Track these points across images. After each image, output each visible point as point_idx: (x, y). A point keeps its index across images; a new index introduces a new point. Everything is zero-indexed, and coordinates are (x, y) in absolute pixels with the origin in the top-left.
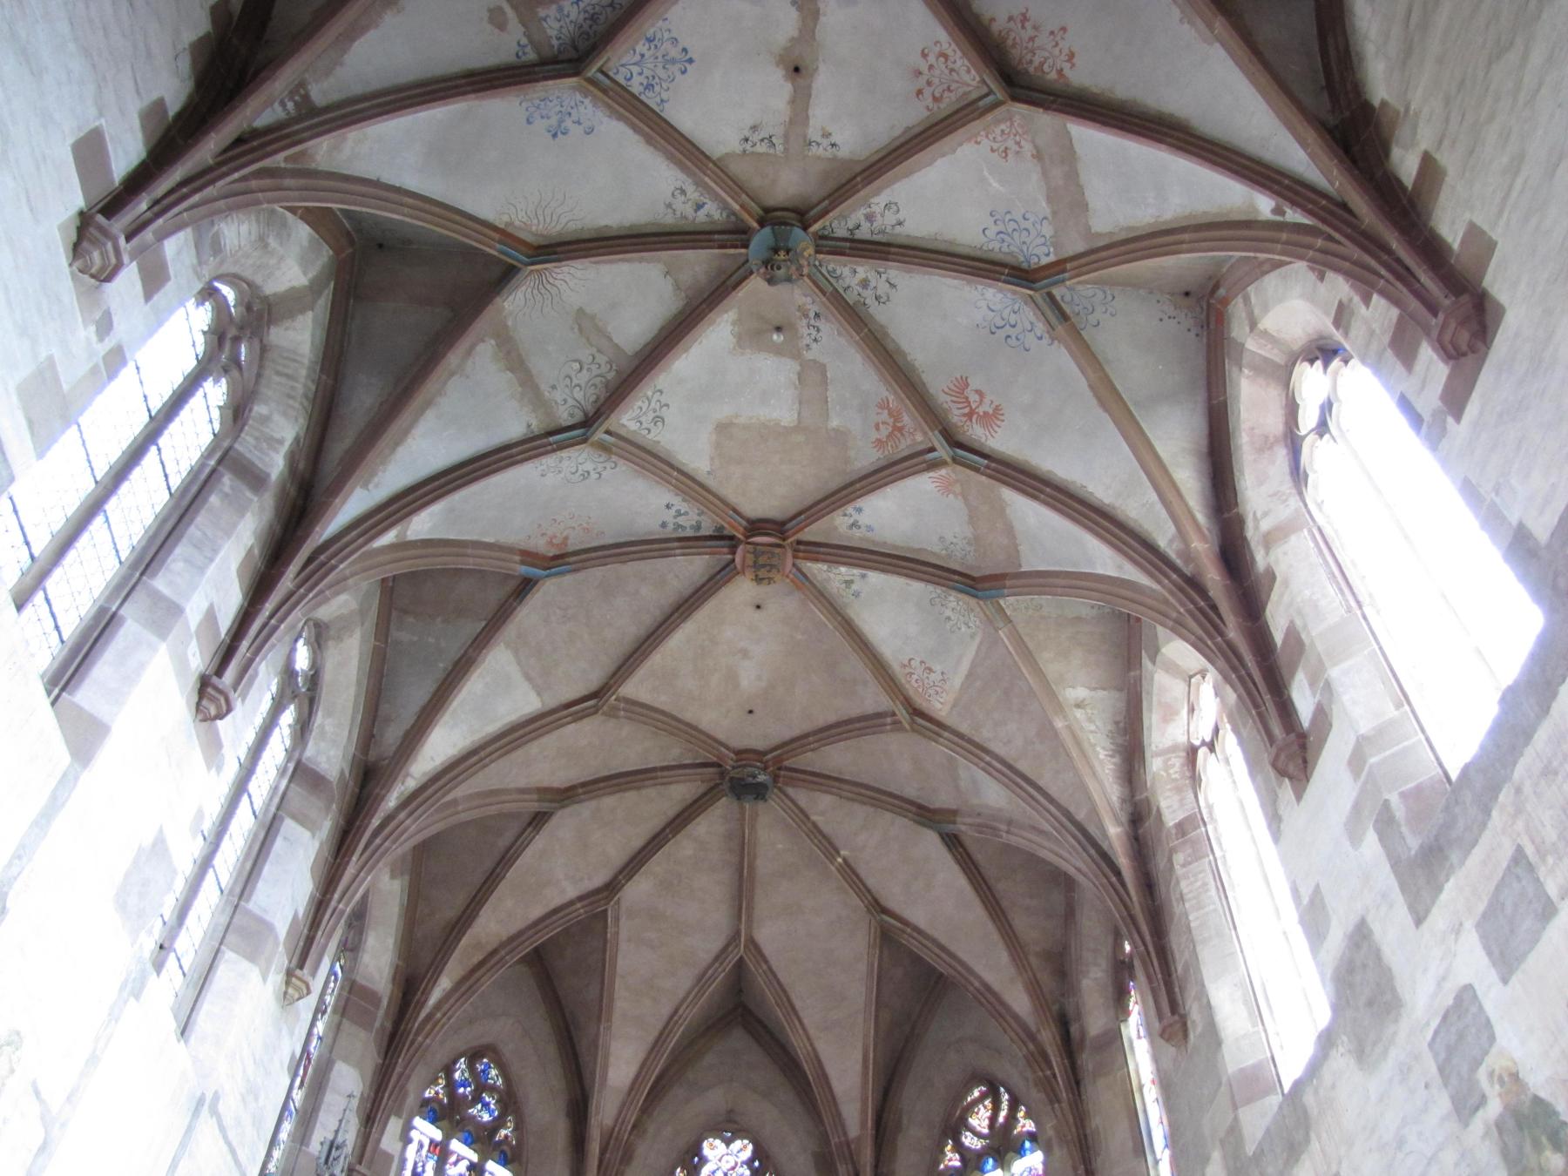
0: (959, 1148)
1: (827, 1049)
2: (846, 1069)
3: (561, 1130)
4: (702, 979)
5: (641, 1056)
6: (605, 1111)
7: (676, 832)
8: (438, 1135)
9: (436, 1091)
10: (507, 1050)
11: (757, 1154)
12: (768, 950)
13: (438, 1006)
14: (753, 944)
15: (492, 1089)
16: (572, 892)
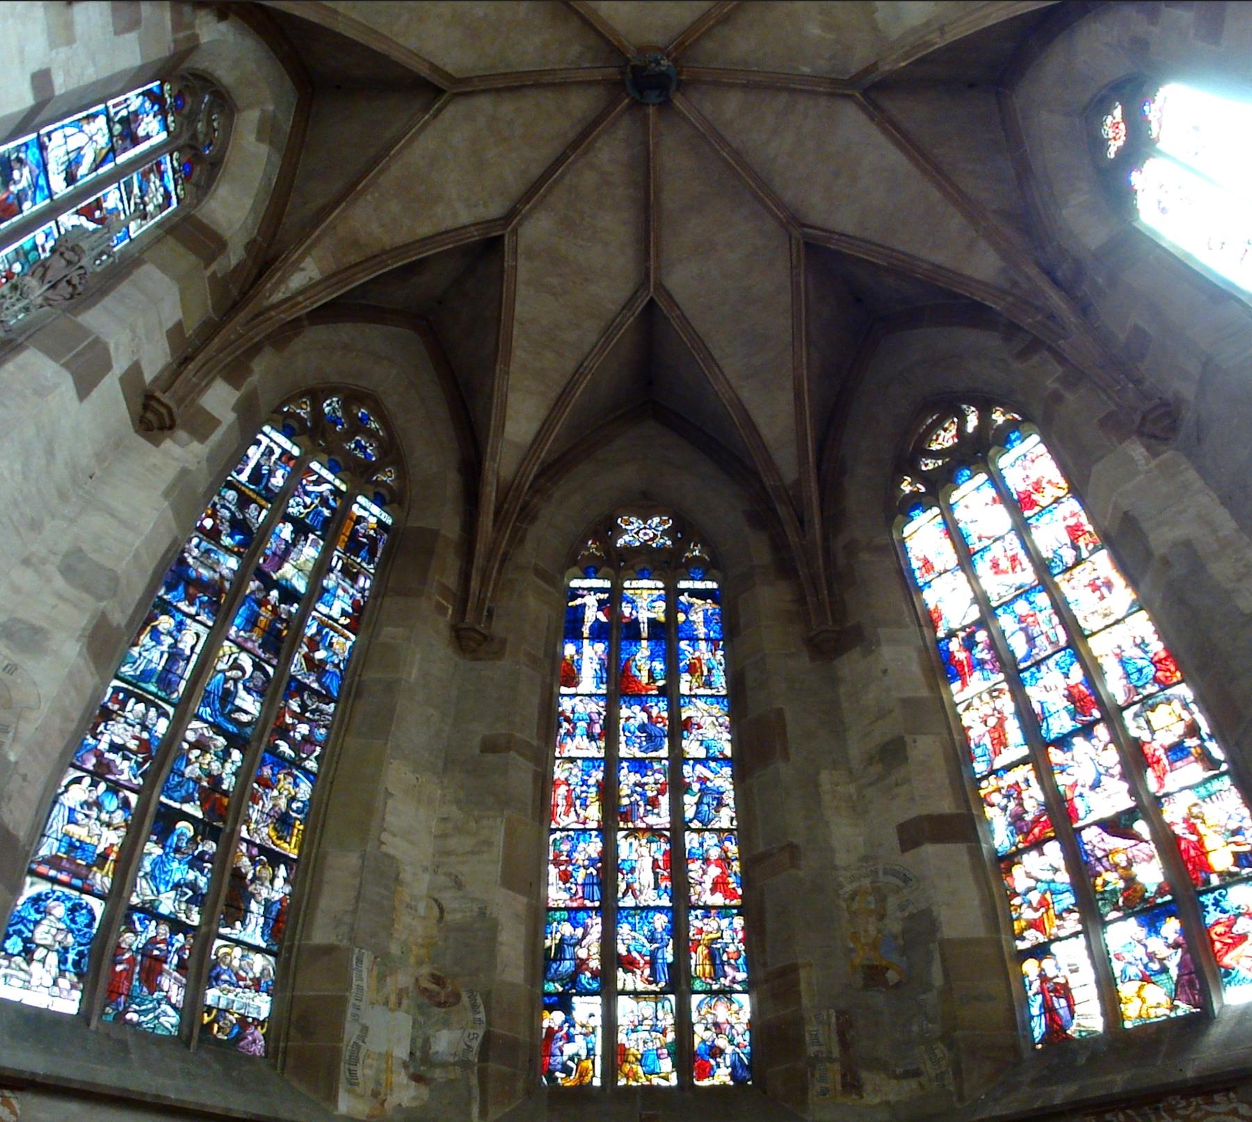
1: (750, 395)
2: (774, 415)
3: (452, 483)
4: (607, 332)
5: (543, 413)
13: (301, 292)
14: (660, 286)
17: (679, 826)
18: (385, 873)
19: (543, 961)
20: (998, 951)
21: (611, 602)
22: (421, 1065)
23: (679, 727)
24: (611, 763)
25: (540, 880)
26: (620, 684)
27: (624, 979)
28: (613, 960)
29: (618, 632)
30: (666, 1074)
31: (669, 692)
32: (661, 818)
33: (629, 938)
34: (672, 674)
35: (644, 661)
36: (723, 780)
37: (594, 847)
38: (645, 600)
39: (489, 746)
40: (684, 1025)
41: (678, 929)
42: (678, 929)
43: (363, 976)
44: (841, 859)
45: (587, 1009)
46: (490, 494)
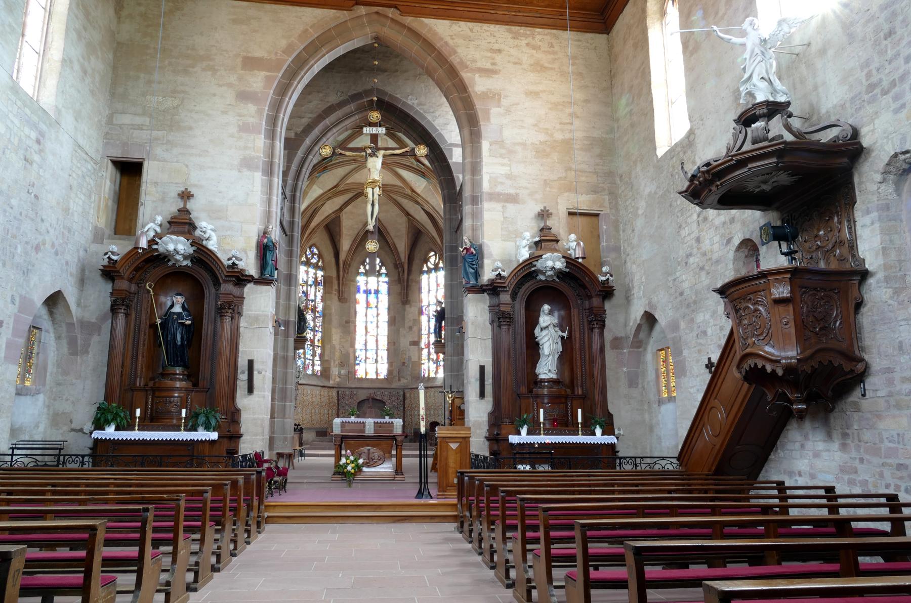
1: (396, 241)
2: (402, 246)
3: (333, 260)
6: (343, 256)
7: (357, 198)
10: (318, 244)
16: (331, 212)
18: (333, 347)
20: (419, 364)
21: (367, 283)
22: (340, 375)
23: (378, 315)
28: (366, 358)
29: (367, 292)
30: (374, 377)
31: (376, 307)
35: (372, 297)
37: (364, 338)
38: (373, 282)
41: (377, 353)
42: (377, 353)
43: (332, 364)
45: (362, 365)
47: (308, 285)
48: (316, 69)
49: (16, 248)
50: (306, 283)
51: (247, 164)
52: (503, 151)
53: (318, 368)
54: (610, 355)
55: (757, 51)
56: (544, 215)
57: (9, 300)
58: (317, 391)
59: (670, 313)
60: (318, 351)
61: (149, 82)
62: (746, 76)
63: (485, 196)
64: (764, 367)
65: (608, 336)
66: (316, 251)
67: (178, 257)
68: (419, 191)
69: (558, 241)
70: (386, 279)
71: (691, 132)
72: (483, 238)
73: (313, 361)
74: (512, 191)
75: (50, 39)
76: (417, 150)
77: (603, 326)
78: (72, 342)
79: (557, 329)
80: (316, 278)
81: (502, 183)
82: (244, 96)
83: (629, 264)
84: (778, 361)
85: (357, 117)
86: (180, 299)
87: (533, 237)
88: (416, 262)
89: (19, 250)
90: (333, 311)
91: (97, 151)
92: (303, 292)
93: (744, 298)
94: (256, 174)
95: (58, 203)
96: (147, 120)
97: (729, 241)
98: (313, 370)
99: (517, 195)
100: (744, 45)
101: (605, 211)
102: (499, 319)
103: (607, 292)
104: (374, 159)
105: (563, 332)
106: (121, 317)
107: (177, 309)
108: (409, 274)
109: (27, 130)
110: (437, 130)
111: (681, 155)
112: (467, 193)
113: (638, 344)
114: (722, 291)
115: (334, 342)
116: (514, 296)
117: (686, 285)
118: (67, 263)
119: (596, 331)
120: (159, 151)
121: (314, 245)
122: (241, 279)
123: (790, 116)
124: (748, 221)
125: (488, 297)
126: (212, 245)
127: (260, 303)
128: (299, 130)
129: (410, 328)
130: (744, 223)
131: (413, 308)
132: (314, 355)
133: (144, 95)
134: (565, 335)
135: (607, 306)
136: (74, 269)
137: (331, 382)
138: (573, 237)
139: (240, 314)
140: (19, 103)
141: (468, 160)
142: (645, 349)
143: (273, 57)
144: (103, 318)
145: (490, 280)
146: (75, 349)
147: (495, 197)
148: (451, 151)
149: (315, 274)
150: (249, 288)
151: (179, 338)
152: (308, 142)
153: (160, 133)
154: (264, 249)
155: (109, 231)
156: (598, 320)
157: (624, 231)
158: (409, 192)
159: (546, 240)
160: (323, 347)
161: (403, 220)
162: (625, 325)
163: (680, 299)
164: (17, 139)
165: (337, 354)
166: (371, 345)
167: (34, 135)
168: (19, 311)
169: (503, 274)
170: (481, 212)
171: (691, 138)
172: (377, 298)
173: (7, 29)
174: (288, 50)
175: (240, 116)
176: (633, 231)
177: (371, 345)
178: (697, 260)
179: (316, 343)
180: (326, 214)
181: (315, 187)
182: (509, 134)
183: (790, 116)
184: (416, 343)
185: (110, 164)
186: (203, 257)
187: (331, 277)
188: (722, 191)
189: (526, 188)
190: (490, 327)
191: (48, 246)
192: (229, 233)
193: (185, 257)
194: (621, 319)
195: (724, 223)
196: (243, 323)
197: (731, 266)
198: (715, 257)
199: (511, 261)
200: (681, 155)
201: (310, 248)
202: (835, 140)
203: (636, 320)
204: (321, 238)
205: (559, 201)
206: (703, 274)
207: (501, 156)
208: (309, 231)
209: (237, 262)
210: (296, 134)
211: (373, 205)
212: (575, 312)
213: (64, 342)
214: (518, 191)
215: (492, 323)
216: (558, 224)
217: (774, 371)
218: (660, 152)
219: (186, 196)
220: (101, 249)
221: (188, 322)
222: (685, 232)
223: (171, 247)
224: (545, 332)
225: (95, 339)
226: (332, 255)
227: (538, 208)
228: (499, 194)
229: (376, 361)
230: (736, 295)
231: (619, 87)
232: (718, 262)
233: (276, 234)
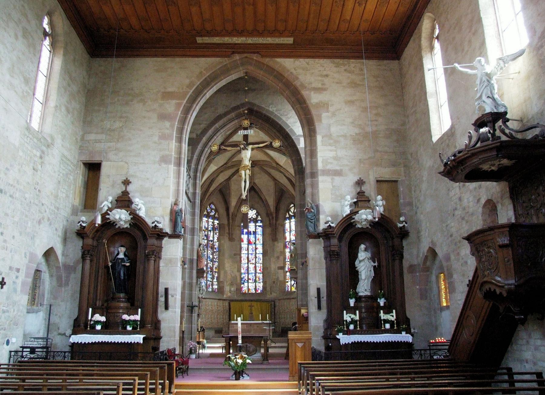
0: (289, 214)
1: (267, 198)
2: (271, 201)
3: (225, 213)
6: (232, 210)
8: (207, 219)
9: (205, 213)
10: (215, 202)
11: (257, 212)
12: (257, 183)
14: (254, 183)
15: (213, 209)
16: (223, 180)
17: (256, 262)
18: (226, 272)
19: (241, 279)
22: (230, 291)
23: (256, 249)
24: (248, 254)
25: (241, 269)
26: (249, 242)
27: (250, 281)
28: (249, 279)
29: (249, 233)
30: (254, 291)
31: (255, 243)
32: (254, 262)
33: (250, 276)
34: (255, 241)
35: (252, 238)
36: (261, 256)
37: (247, 265)
39: (235, 255)
40: (256, 286)
41: (255, 275)
42: (255, 275)
44: (272, 269)
45: (246, 284)
46: (231, 214)
47: (208, 231)
48: (208, 95)
49: (27, 223)
50: (207, 229)
51: (164, 160)
52: (332, 141)
53: (215, 287)
54: (407, 278)
55: (484, 79)
56: (360, 183)
57: (23, 255)
58: (215, 302)
59: (445, 249)
60: (216, 275)
61: (106, 113)
62: (478, 95)
63: (319, 173)
64: (495, 290)
65: (406, 264)
66: (213, 207)
67: (122, 223)
68: (281, 164)
69: (369, 201)
70: (261, 224)
71: (452, 127)
72: (319, 201)
73: (212, 282)
74: (338, 168)
75: (49, 94)
76: (273, 144)
77: (402, 257)
78: (59, 279)
79: (370, 261)
80: (214, 225)
81: (331, 163)
82: (163, 117)
83: (418, 214)
84: (503, 287)
85: (236, 121)
86: (123, 249)
87: (352, 199)
88: (282, 211)
89: (29, 225)
90: (226, 247)
91: (75, 157)
92: (205, 235)
93: (482, 243)
94: (170, 166)
95: (52, 193)
96: (103, 137)
97: (479, 200)
98: (212, 288)
99: (341, 170)
100: (475, 75)
101: (401, 178)
102: (330, 255)
103: (404, 234)
104: (246, 151)
105: (374, 262)
106: (88, 262)
107: (121, 256)
108: (276, 220)
109: (35, 151)
110: (289, 127)
111: (447, 141)
112: (308, 171)
113: (427, 269)
114: (469, 238)
115: (227, 269)
116: (340, 239)
117: (453, 230)
118: (56, 229)
119: (397, 262)
120: (111, 156)
121: (212, 203)
122: (160, 235)
123: (508, 120)
124: (489, 189)
125: (323, 241)
126: (142, 213)
127: (173, 250)
128: (199, 132)
129: (278, 258)
130: (487, 189)
131: (280, 244)
132: (213, 278)
133: (102, 121)
134: (376, 264)
135: (405, 243)
136: (60, 233)
137: (225, 296)
138: (379, 197)
139: (160, 258)
140: (30, 136)
141: (308, 148)
142: (432, 273)
143: (181, 91)
144: (77, 263)
145: (323, 229)
146: (61, 282)
147: (327, 172)
148: (299, 140)
149: (213, 223)
150: (166, 240)
151: (122, 275)
152: (204, 139)
153: (111, 144)
154: (175, 216)
155: (80, 208)
156: (398, 254)
157: (415, 192)
158: (274, 165)
159: (361, 200)
160: (219, 273)
161: (271, 183)
162: (418, 256)
163: (450, 239)
164: (29, 157)
165: (229, 277)
166: (252, 270)
167: (38, 154)
168: (29, 262)
169: (332, 225)
170: (317, 184)
171: (453, 131)
172: (255, 238)
173: (25, 94)
174: (189, 86)
175: (160, 129)
176: (420, 191)
177: (252, 270)
178: (460, 213)
179: (214, 270)
180: (220, 182)
181: (212, 165)
182: (335, 130)
183: (508, 120)
184: (283, 268)
185: (82, 165)
186: (137, 222)
187: (223, 224)
188: (467, 170)
189: (347, 165)
190: (324, 261)
191: (46, 220)
192: (153, 205)
193: (126, 222)
194: (415, 252)
195: (475, 188)
196: (162, 264)
197: (480, 218)
198: (471, 210)
199: (338, 216)
200: (447, 141)
201: (210, 205)
202: (536, 137)
203: (423, 253)
204: (217, 199)
205: (371, 173)
206: (464, 222)
207: (330, 145)
208: (208, 194)
209: (158, 225)
210: (197, 135)
211: (245, 182)
212: (382, 248)
213: (55, 279)
214: (342, 168)
215: (326, 258)
216: (369, 189)
217: (501, 293)
218: (435, 138)
219: (127, 183)
220: (76, 219)
221: (128, 264)
222: (452, 193)
223: (117, 217)
224: (362, 264)
225: (72, 276)
226: (225, 209)
227: (356, 179)
228: (329, 171)
229: (255, 281)
230: (477, 241)
231: (405, 99)
232: (472, 214)
233: (184, 204)
